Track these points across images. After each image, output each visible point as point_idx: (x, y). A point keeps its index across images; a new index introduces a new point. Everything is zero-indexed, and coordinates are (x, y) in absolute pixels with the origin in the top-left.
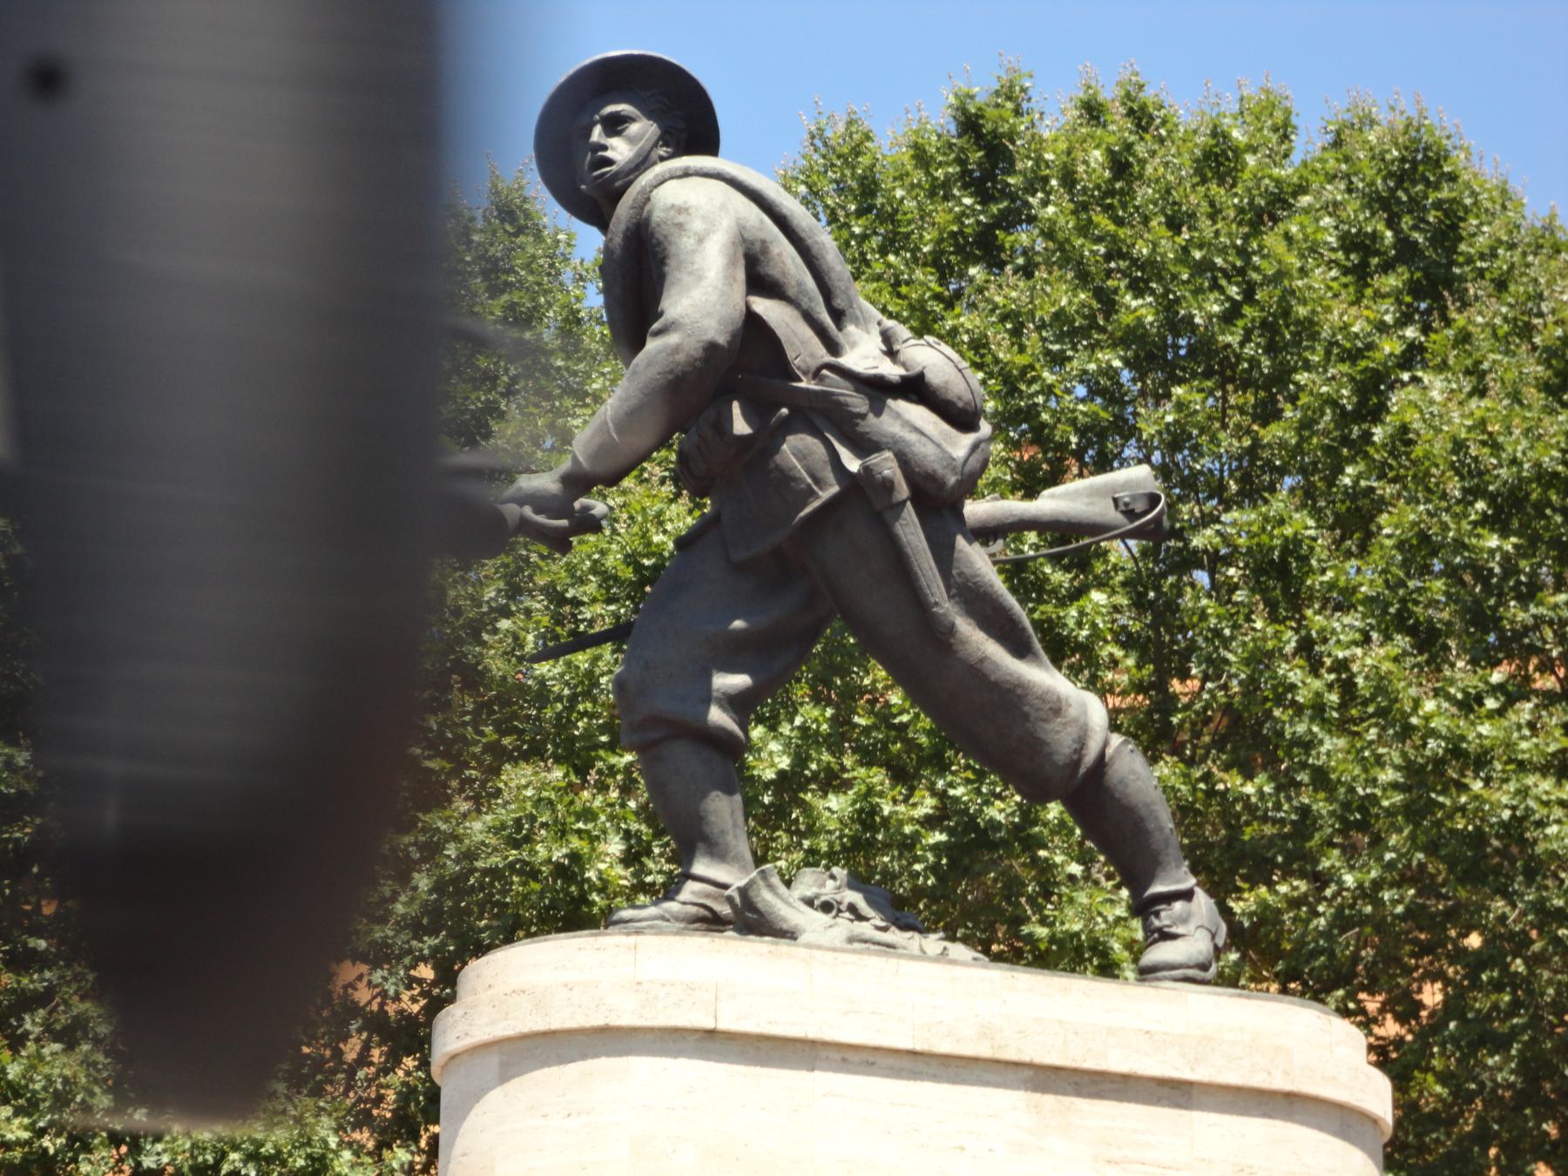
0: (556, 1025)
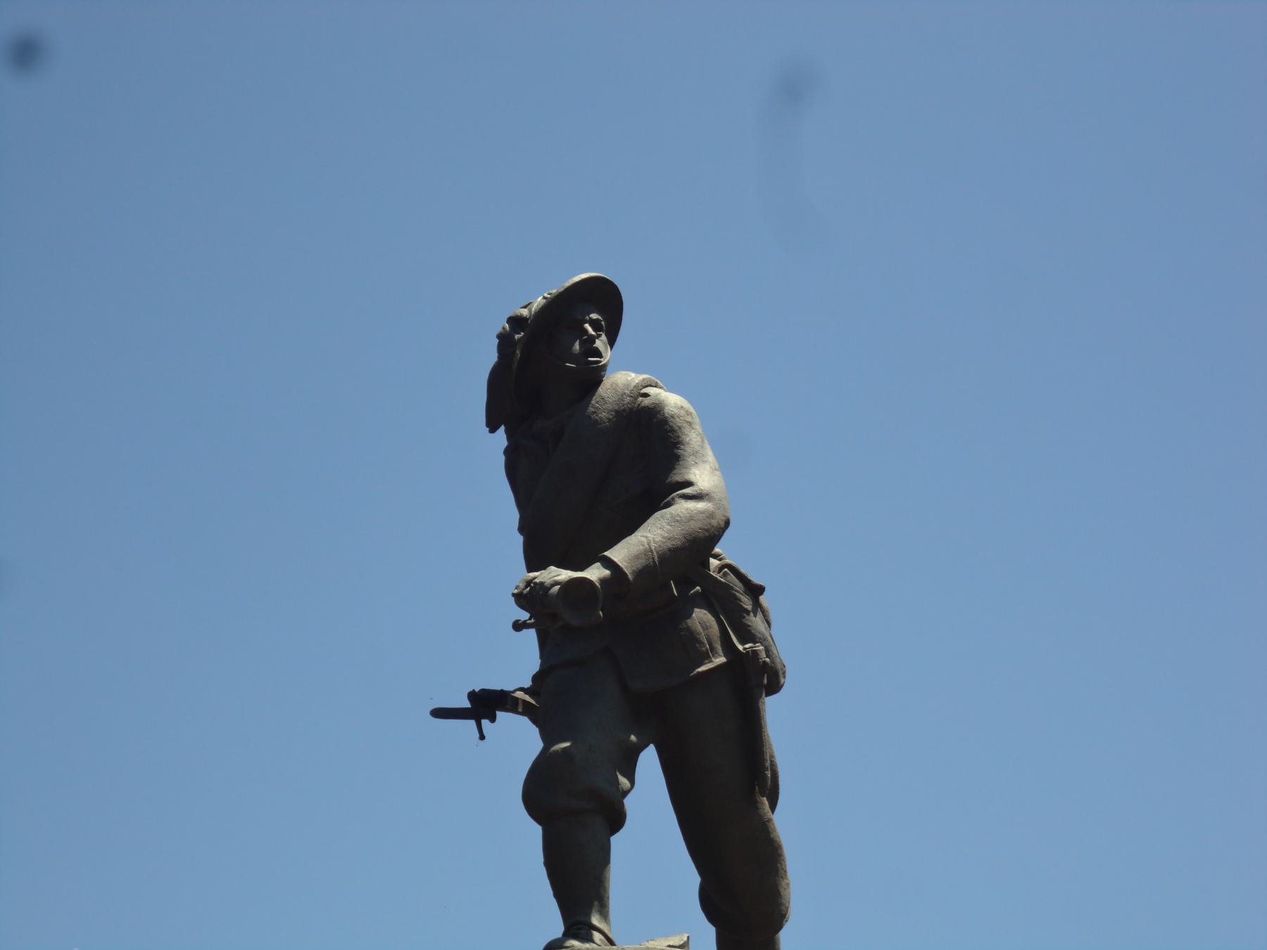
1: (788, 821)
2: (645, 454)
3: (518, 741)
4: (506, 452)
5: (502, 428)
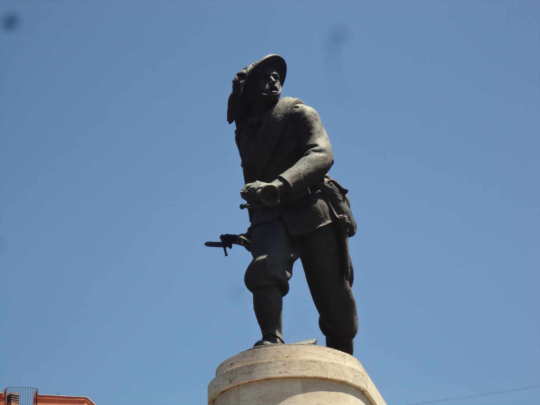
0: (330, 376)
1: (358, 291)
2: (297, 133)
3: (241, 257)
4: (236, 132)
5: (234, 122)
